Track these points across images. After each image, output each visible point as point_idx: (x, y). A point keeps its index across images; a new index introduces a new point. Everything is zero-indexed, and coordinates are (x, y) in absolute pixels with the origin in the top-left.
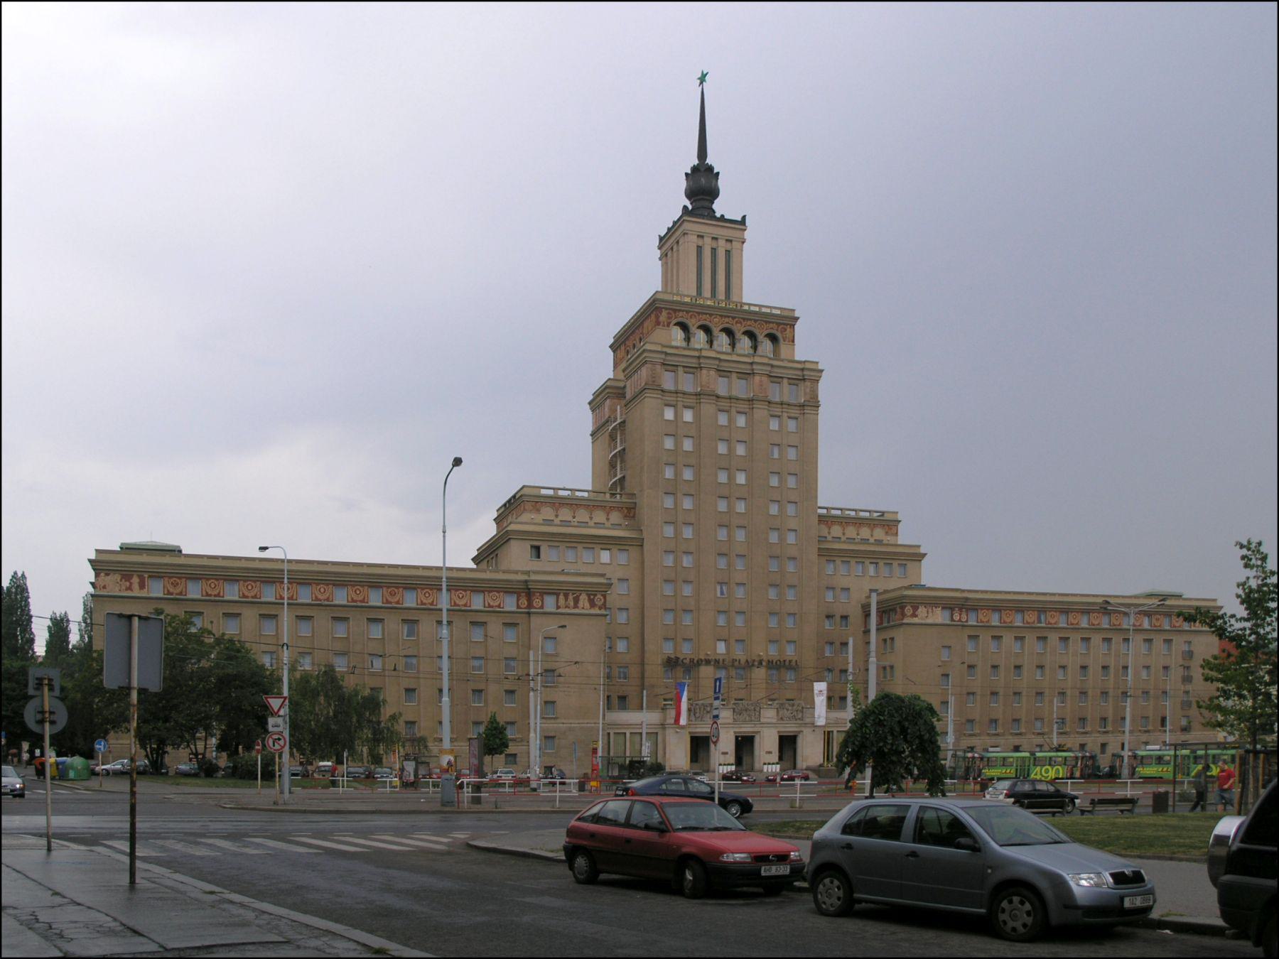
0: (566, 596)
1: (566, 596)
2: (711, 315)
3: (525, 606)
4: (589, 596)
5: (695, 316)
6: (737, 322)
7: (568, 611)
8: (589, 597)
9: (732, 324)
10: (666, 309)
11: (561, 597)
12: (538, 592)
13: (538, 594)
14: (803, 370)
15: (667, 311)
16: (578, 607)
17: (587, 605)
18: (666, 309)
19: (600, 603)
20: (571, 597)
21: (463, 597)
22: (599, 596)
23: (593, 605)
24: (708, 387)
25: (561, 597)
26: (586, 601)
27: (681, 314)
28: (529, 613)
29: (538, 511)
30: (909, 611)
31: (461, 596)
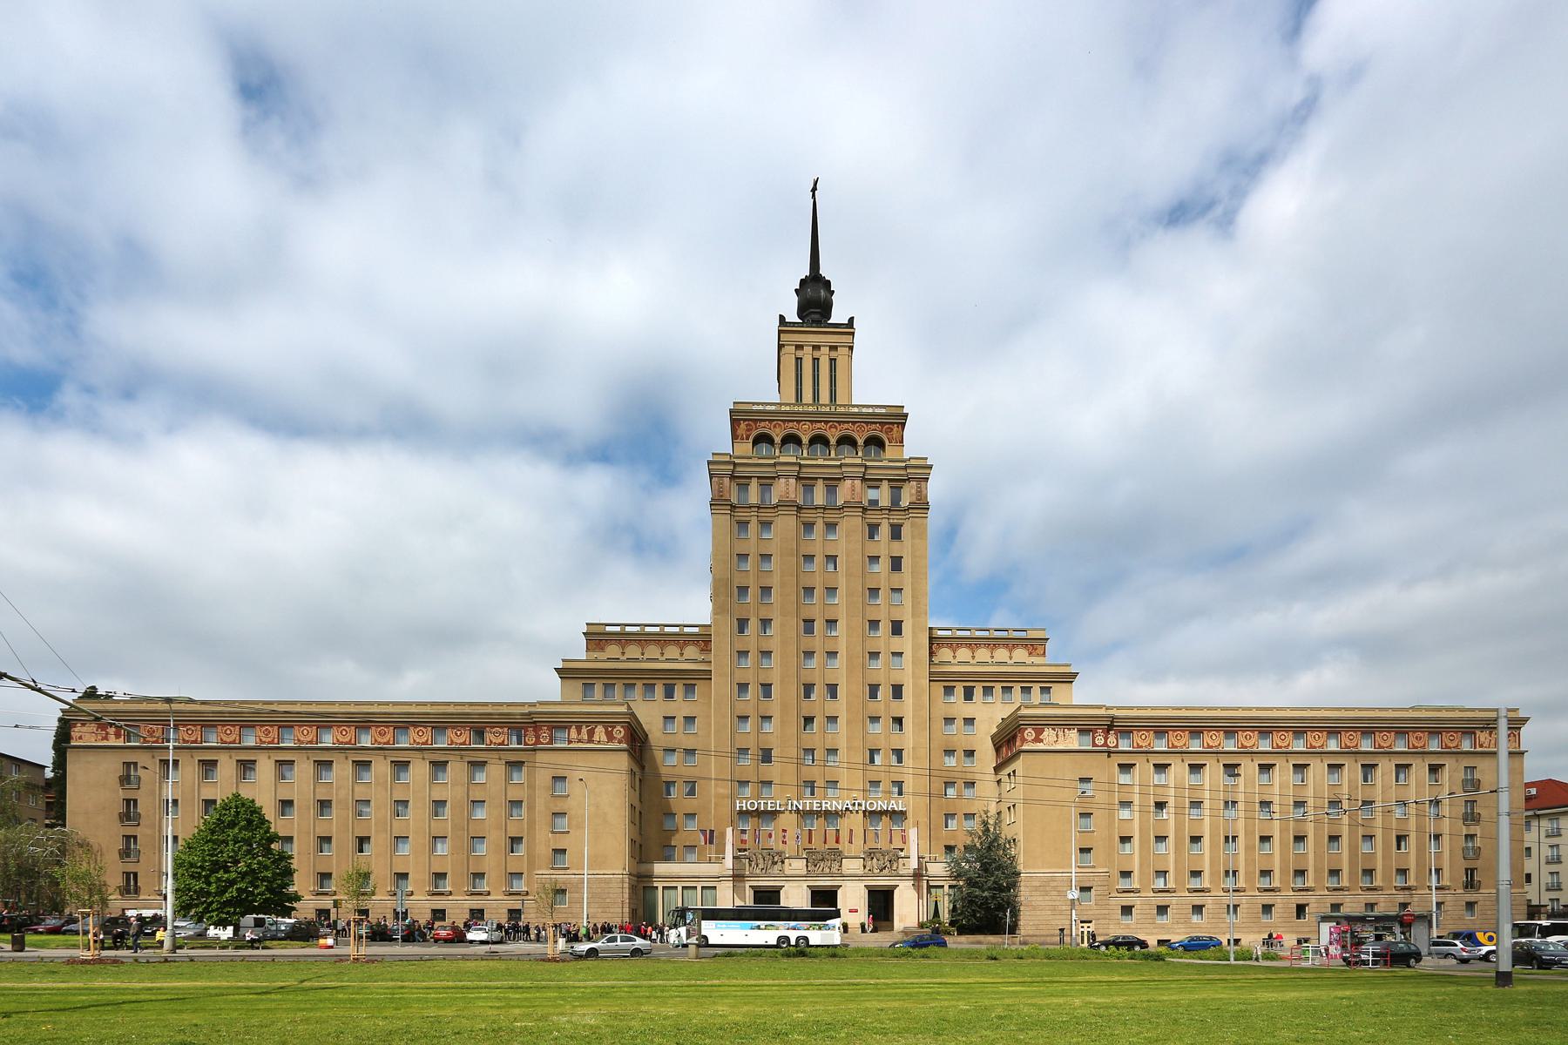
2: (798, 422)
5: (780, 425)
6: (831, 427)
7: (581, 745)
9: (825, 430)
10: (745, 420)
11: (573, 731)
14: (906, 468)
15: (747, 423)
17: (604, 738)
18: (745, 420)
20: (584, 730)
21: (461, 734)
23: (610, 737)
24: (788, 497)
25: (573, 731)
27: (763, 424)
28: (535, 750)
29: (602, 649)
30: (1029, 733)
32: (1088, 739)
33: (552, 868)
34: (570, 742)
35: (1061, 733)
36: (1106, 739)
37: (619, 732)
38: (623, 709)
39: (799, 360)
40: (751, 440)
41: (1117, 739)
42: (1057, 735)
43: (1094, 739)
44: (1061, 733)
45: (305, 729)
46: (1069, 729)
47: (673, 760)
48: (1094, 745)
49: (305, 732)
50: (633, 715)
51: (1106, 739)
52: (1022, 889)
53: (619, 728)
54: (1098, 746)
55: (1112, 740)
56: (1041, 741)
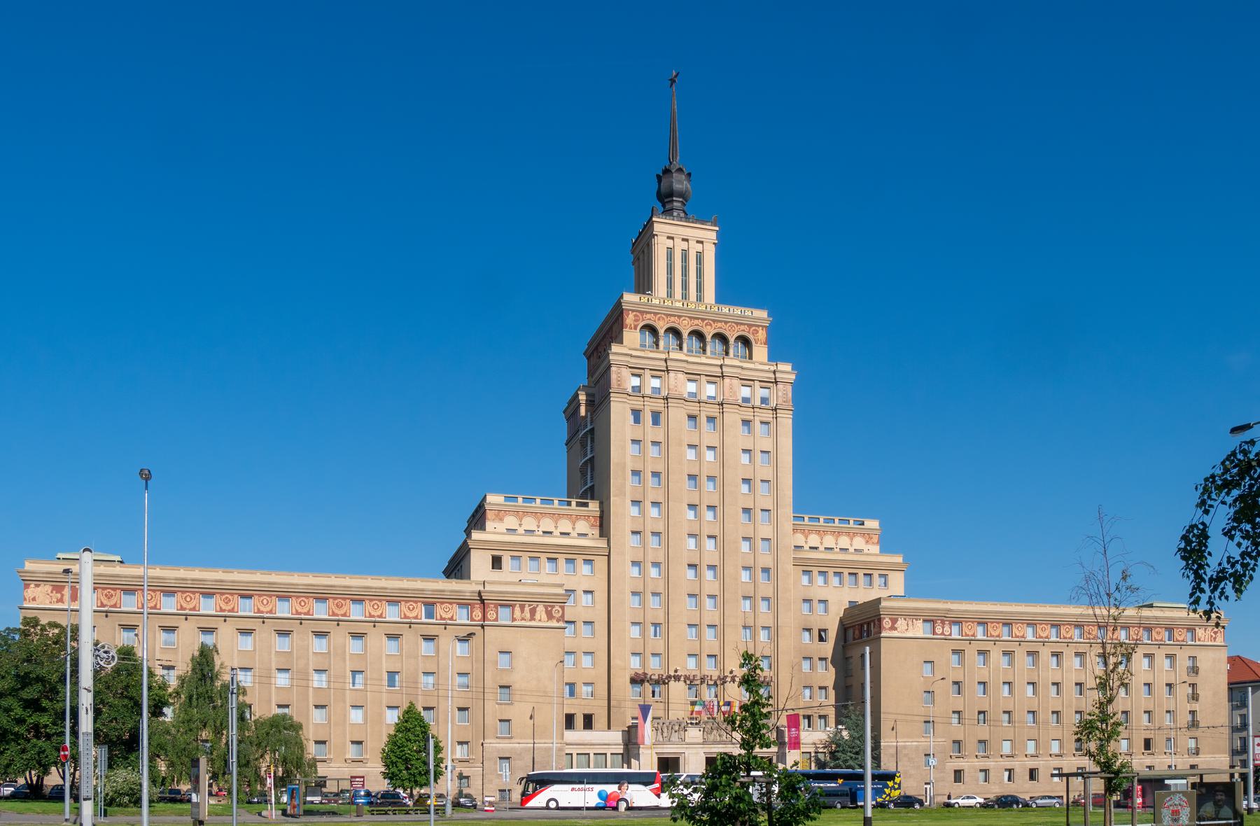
0: (522, 608)
1: (522, 608)
2: (679, 317)
3: (479, 618)
4: (546, 607)
5: (663, 319)
6: (706, 325)
7: (523, 623)
8: (546, 609)
9: (702, 327)
10: (633, 311)
11: (517, 609)
12: (492, 604)
13: (493, 606)
15: (635, 313)
16: (534, 620)
17: (544, 616)
18: (633, 311)
19: (558, 615)
20: (527, 609)
21: (413, 608)
22: (557, 608)
23: (550, 616)
24: (676, 391)
25: (517, 609)
26: (544, 613)
29: (501, 520)
31: (411, 607)
34: (514, 619)
35: (910, 623)
40: (638, 330)
41: (951, 628)
44: (910, 623)
46: (917, 620)
51: (943, 628)
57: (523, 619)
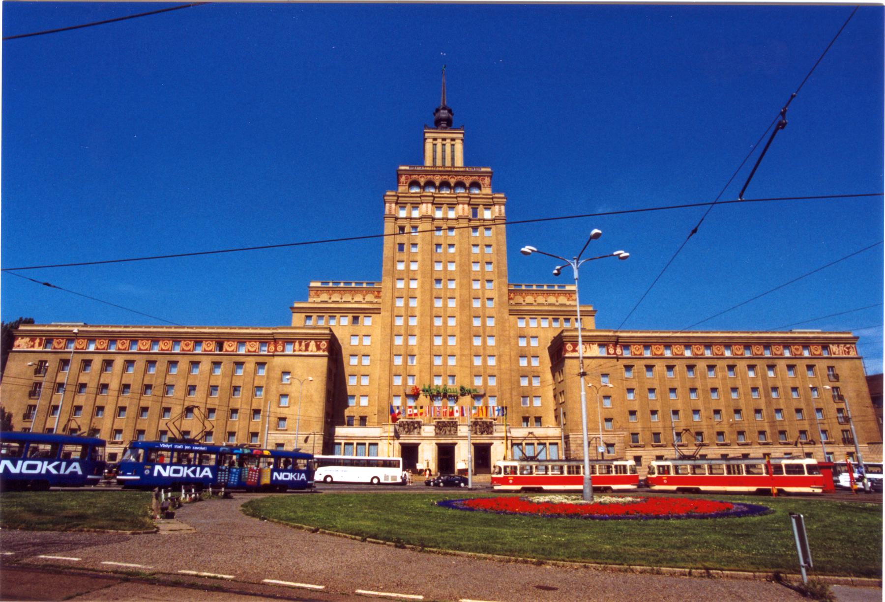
4: (316, 343)
7: (300, 353)
11: (297, 344)
17: (314, 349)
20: (303, 344)
23: (318, 348)
25: (297, 344)
32: (604, 350)
33: (277, 430)
35: (588, 346)
36: (615, 350)
37: (324, 345)
38: (327, 332)
39: (435, 145)
41: (622, 350)
42: (586, 348)
43: (608, 350)
45: (144, 342)
46: (593, 344)
47: (354, 361)
48: (608, 353)
49: (144, 344)
50: (333, 335)
51: (615, 350)
52: (571, 445)
53: (324, 342)
54: (610, 354)
55: (619, 351)
56: (576, 351)
57: (300, 350)
